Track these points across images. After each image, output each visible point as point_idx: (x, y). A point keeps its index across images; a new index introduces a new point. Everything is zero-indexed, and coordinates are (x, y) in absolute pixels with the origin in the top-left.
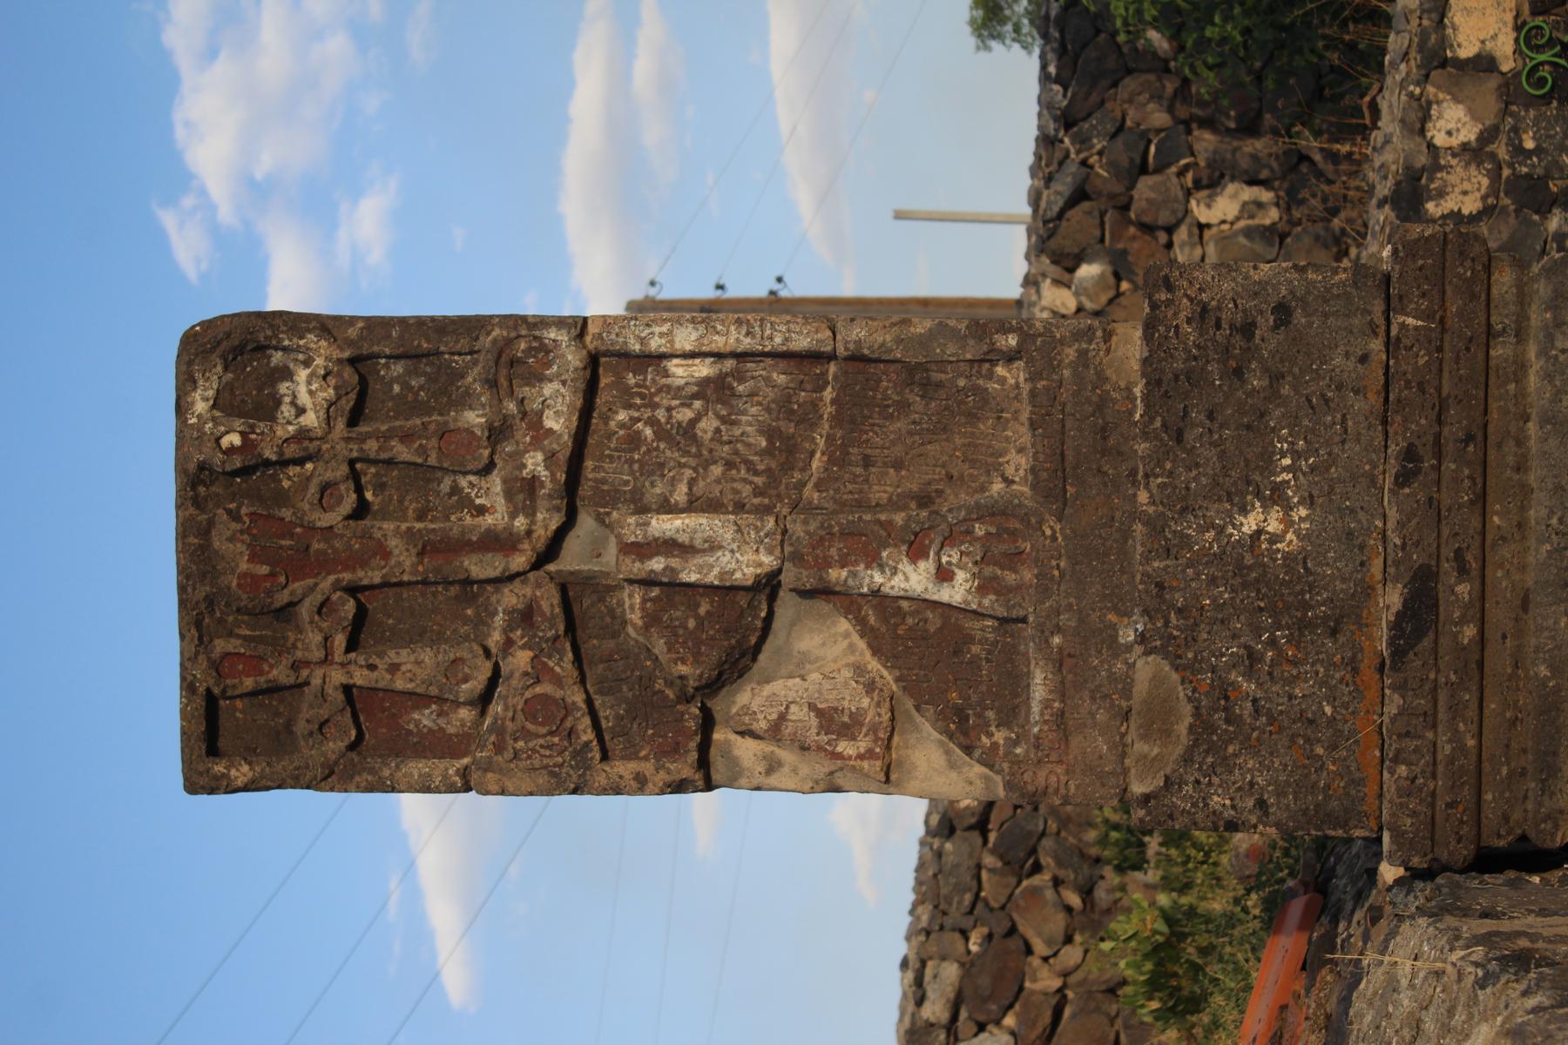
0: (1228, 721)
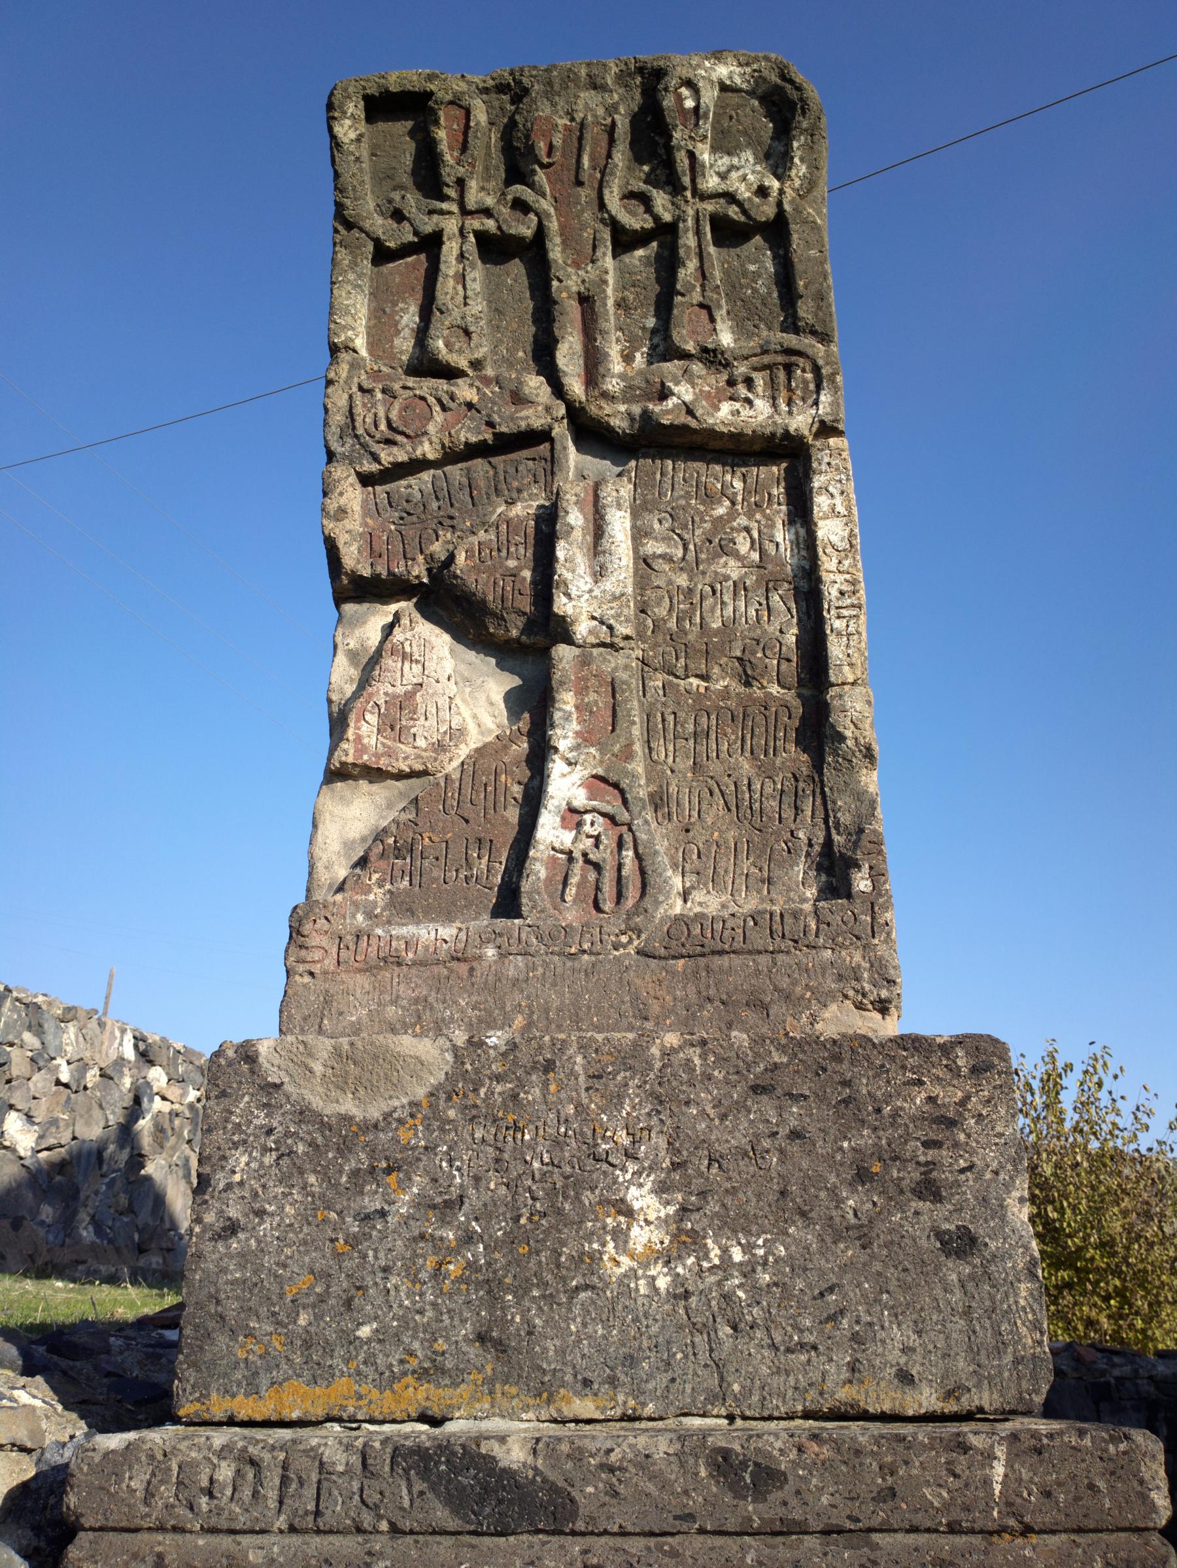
0: (356, 1173)
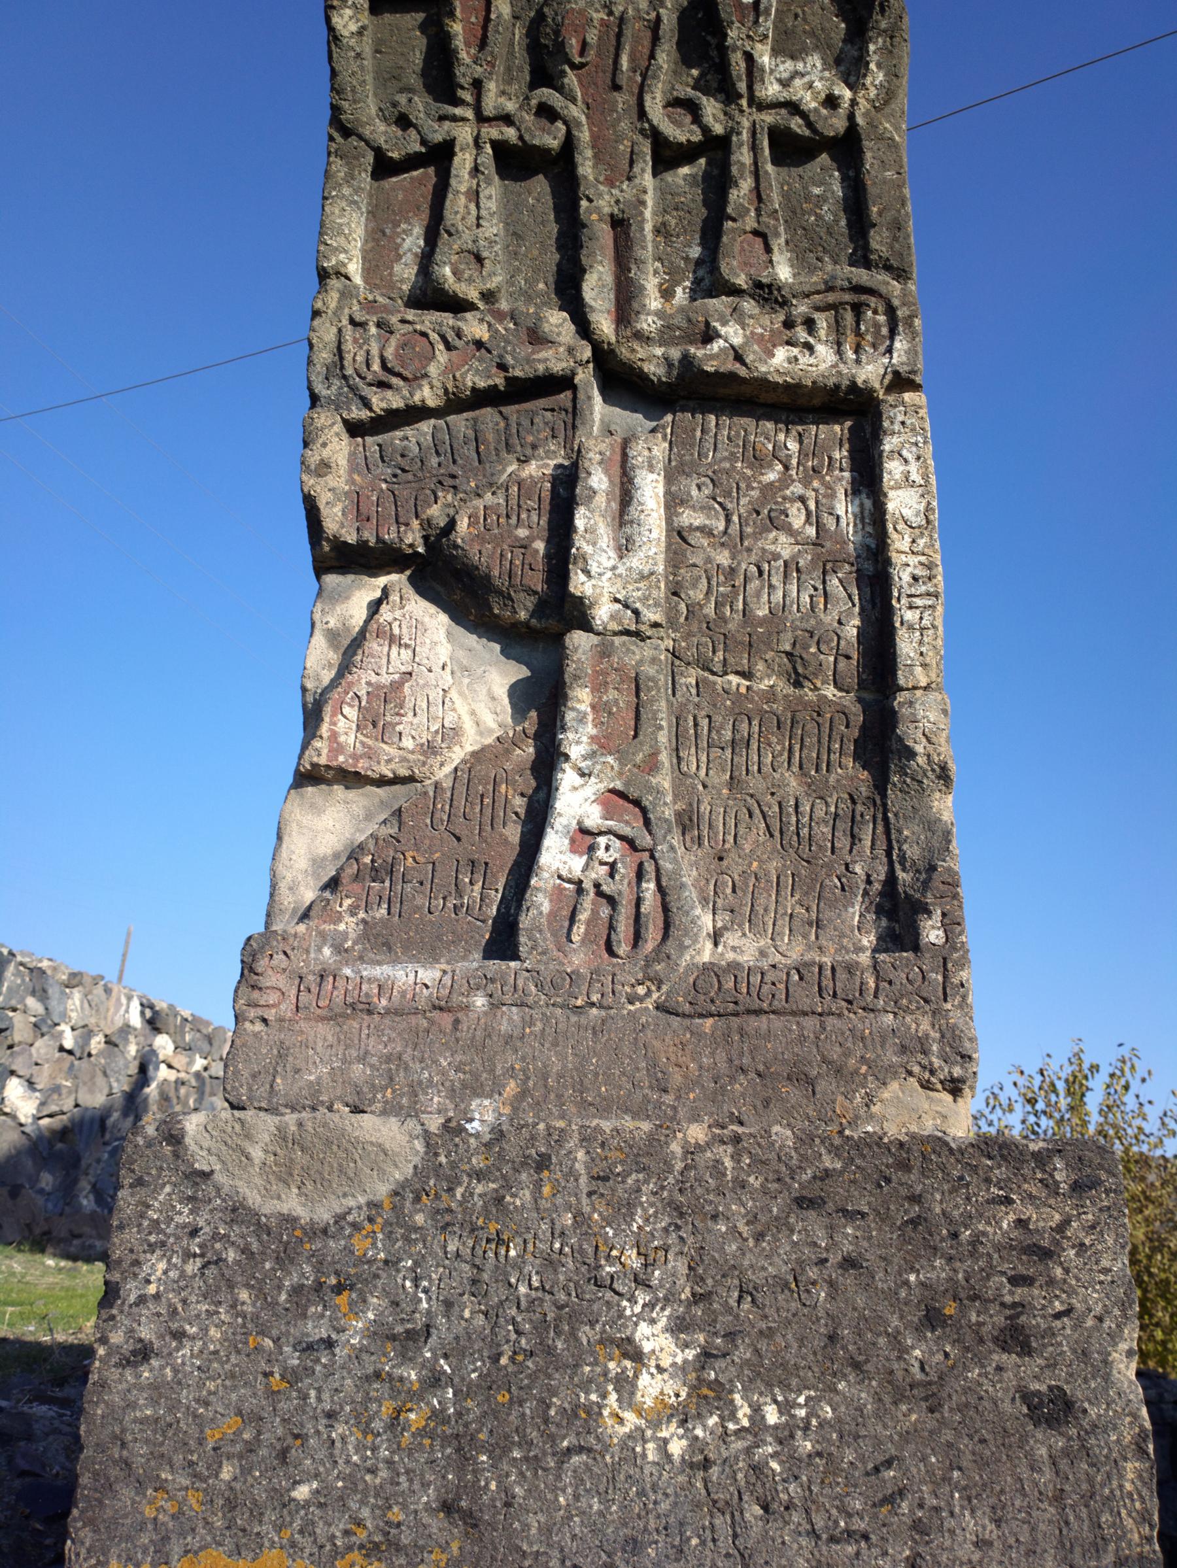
0: (297, 1290)
